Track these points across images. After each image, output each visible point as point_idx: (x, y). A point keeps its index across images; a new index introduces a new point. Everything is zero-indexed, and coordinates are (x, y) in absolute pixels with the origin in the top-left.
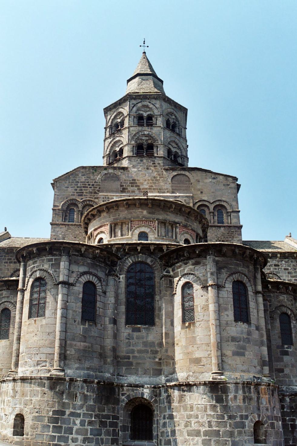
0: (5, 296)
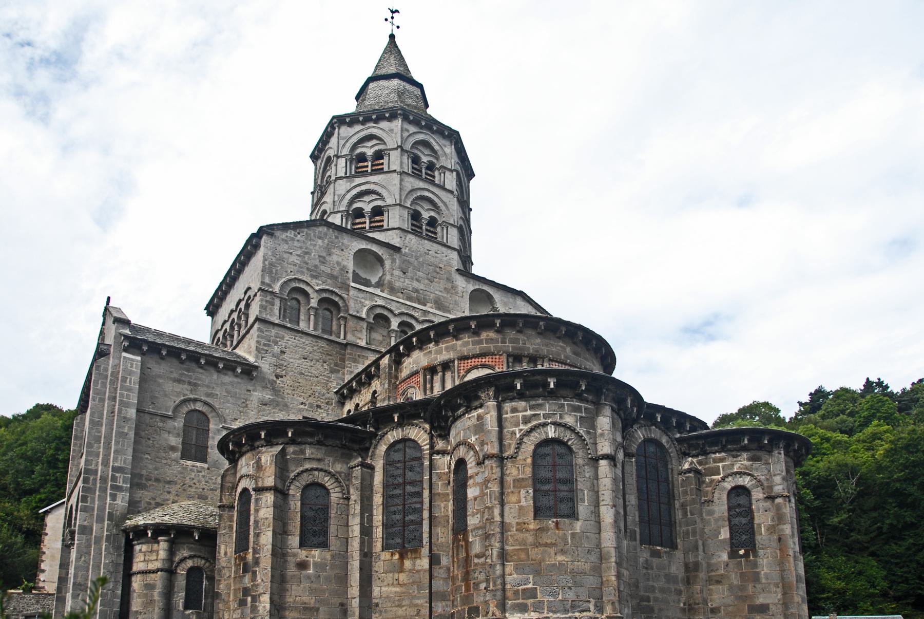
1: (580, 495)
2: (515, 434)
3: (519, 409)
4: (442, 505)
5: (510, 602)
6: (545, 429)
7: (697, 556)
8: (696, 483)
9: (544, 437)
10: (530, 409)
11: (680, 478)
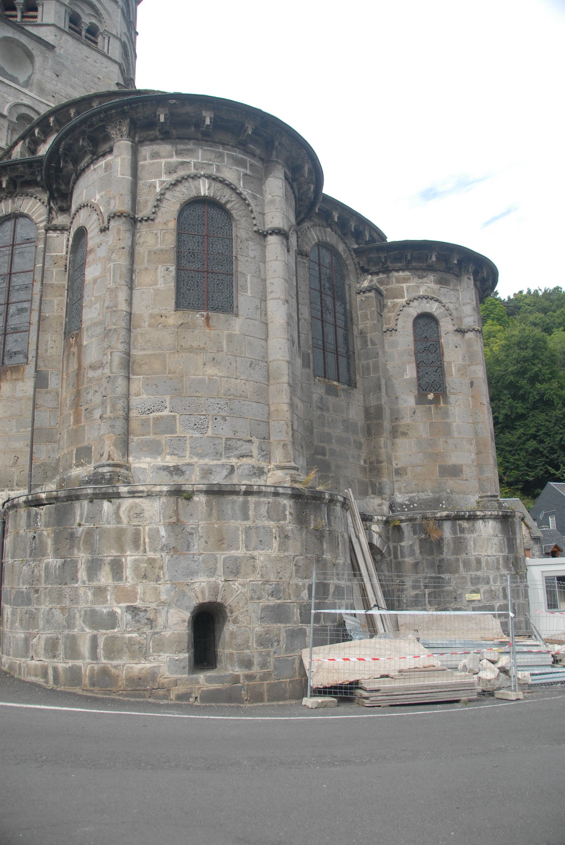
1: (241, 281)
2: (155, 187)
3: (161, 154)
5: (135, 439)
6: (196, 183)
7: (379, 398)
8: (377, 305)
9: (194, 194)
10: (176, 154)
11: (359, 298)
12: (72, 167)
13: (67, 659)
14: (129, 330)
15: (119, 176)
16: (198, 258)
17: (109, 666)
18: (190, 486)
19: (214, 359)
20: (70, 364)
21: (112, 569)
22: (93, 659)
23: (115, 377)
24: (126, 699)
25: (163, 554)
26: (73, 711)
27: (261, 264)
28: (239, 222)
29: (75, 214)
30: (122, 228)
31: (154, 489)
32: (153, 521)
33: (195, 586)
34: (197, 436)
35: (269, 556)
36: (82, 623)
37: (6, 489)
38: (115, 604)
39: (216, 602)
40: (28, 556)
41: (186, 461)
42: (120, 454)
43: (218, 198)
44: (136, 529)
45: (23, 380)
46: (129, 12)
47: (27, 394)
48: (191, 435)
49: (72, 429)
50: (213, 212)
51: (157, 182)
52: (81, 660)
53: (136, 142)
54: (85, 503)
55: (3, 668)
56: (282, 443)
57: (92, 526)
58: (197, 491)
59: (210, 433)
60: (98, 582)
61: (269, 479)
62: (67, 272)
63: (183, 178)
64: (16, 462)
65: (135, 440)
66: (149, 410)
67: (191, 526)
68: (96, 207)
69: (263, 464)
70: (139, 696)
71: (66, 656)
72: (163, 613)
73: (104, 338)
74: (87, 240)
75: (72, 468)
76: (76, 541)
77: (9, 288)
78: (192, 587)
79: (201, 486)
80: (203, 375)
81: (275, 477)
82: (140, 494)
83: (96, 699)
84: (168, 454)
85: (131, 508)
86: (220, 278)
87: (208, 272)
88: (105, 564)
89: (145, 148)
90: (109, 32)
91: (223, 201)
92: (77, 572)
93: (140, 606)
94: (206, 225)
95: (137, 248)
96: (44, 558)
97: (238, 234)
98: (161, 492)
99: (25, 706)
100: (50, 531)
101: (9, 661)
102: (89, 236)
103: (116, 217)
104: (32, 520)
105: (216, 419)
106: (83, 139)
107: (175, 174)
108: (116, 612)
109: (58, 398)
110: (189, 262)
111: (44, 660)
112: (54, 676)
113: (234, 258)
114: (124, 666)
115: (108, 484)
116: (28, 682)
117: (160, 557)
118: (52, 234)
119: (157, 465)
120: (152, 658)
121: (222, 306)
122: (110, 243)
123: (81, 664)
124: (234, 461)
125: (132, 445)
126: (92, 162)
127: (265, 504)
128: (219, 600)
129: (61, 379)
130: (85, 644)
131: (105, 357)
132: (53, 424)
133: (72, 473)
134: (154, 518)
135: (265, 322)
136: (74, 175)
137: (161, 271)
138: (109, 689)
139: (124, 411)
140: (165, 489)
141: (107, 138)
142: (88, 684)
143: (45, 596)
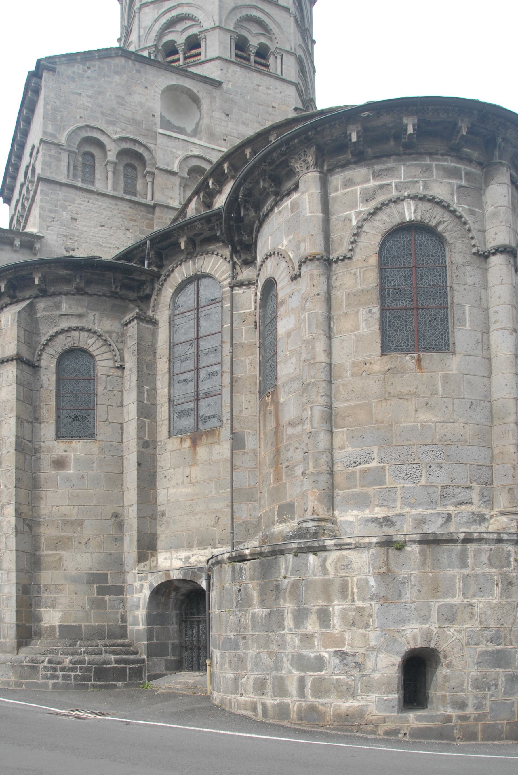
0: (69, 312)
2: (350, 220)
4: (247, 361)
6: (399, 207)
9: (397, 220)
12: (254, 214)
13: (275, 696)
14: (330, 382)
15: (308, 214)
16: (405, 294)
17: (317, 703)
18: (402, 536)
19: (427, 404)
20: (268, 423)
21: (319, 618)
22: (300, 697)
23: (317, 431)
24: (334, 732)
25: (373, 603)
26: (282, 740)
27: (482, 290)
28: (453, 246)
29: (262, 265)
30: (315, 273)
31: (362, 541)
32: (362, 572)
33: (406, 633)
34: (409, 485)
35: (489, 603)
36: (289, 666)
37: (209, 547)
38: (322, 649)
39: (429, 648)
40: (234, 607)
41: (397, 512)
42: (325, 509)
43: (426, 221)
44: (344, 580)
45: (219, 443)
46: (303, 18)
47: (224, 457)
48: (402, 485)
49: (273, 487)
50: (422, 239)
51: (353, 214)
52: (289, 698)
53: (325, 172)
54: (290, 557)
55: (214, 702)
56: (507, 488)
57: (298, 578)
58: (409, 541)
59: (423, 482)
60: (304, 630)
61: (490, 526)
62: (258, 329)
63: (383, 204)
64: (217, 522)
65: (340, 494)
66: (354, 462)
67: (402, 576)
68: (284, 254)
69: (484, 511)
70: (347, 730)
71: (274, 694)
72: (373, 658)
73: (303, 392)
74: (276, 292)
75: (274, 524)
76: (282, 592)
77: (198, 353)
78: (403, 633)
79: (414, 536)
80: (415, 421)
81: (499, 523)
82: (348, 547)
83: (304, 732)
84: (377, 506)
85: (338, 560)
86: (432, 313)
87: (418, 309)
88: (312, 613)
89: (336, 176)
90: (281, 49)
91: (433, 223)
92: (284, 621)
93: (348, 651)
94: (413, 254)
95: (334, 292)
96: (250, 608)
97: (453, 259)
98: (370, 543)
99: (237, 734)
100: (254, 584)
101: (220, 697)
102: (279, 287)
103: (308, 262)
104: (237, 574)
105: (430, 467)
106: (264, 180)
107: (373, 201)
108: (323, 656)
109: (257, 458)
110: (395, 300)
111: (253, 696)
112: (262, 710)
113: (448, 288)
114: (331, 704)
115: (313, 538)
116: (238, 715)
117: (369, 605)
118: (238, 291)
119: (365, 518)
120: (360, 697)
121: (435, 345)
122: (302, 292)
123: (289, 701)
124: (450, 509)
125: (338, 500)
126: (276, 204)
127: (487, 551)
128: (432, 646)
129: (258, 438)
130: (292, 684)
131: (305, 412)
132: (252, 483)
133: (275, 530)
134: (362, 568)
135: (488, 356)
136: (257, 222)
137: (363, 315)
138: (317, 723)
139: (328, 466)
140: (374, 540)
141: (291, 173)
142: (296, 718)
143: (252, 641)
